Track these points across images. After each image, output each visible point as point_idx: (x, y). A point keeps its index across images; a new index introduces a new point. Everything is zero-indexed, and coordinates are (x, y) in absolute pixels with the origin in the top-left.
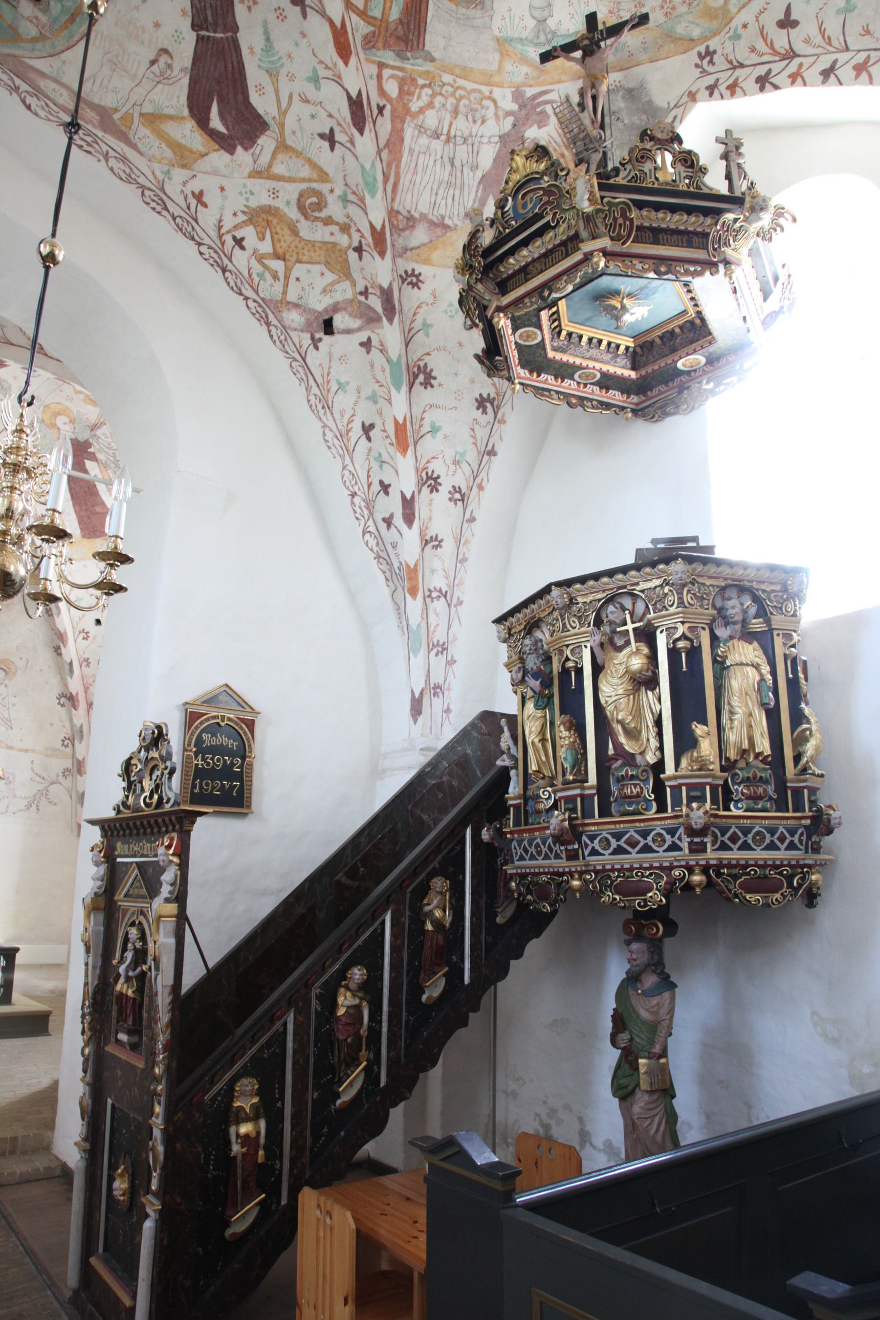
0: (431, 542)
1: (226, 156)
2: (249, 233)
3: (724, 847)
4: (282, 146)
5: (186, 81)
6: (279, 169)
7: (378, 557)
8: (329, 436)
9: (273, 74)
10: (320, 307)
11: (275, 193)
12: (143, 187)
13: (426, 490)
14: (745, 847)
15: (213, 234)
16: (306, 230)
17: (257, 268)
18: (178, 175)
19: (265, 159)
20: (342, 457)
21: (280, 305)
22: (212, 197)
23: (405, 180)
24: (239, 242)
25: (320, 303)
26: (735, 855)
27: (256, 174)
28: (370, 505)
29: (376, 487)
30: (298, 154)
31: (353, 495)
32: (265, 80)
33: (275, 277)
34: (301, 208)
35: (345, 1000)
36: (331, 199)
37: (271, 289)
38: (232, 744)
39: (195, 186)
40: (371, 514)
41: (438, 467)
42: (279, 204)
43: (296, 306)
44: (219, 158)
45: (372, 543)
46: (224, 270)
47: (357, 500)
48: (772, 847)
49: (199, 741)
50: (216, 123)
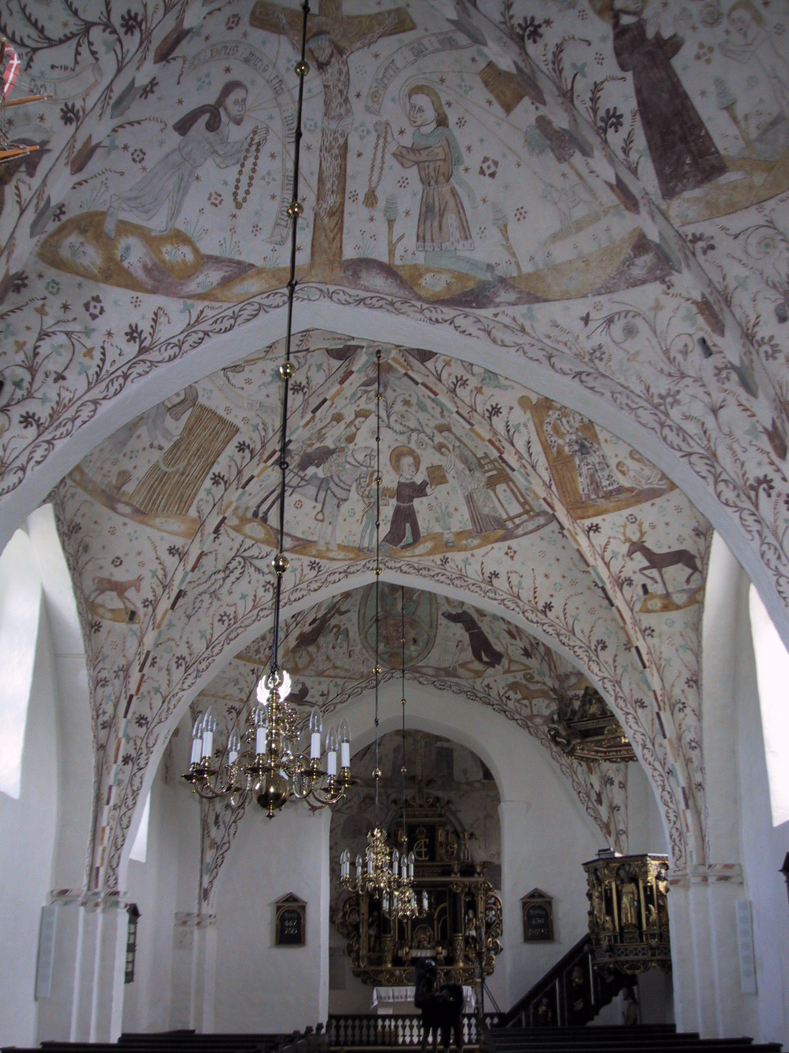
0: (614, 808)
1: (493, 669)
2: (511, 693)
3: (619, 955)
4: (511, 661)
5: (470, 648)
6: (513, 668)
7: (595, 818)
8: (564, 768)
9: (498, 638)
10: (547, 714)
11: (515, 677)
12: (467, 692)
13: (608, 785)
14: (627, 955)
15: (497, 698)
16: (531, 686)
17: (518, 705)
18: (478, 681)
19: (506, 666)
20: (572, 776)
21: (532, 717)
22: (493, 685)
23: (558, 664)
24: (508, 698)
25: (547, 712)
26: (623, 958)
27: (505, 672)
28: (588, 796)
29: (589, 786)
30: (517, 662)
31: (579, 792)
32: (496, 641)
33: (526, 706)
34: (527, 680)
35: (542, 1009)
36: (535, 675)
37: (526, 712)
38: (543, 913)
39: (485, 683)
40: (589, 799)
41: (611, 774)
42: (517, 680)
43: (538, 715)
44: (490, 671)
45: (591, 812)
46: (505, 712)
47: (581, 795)
48: (636, 954)
49: (528, 913)
50: (485, 659)
